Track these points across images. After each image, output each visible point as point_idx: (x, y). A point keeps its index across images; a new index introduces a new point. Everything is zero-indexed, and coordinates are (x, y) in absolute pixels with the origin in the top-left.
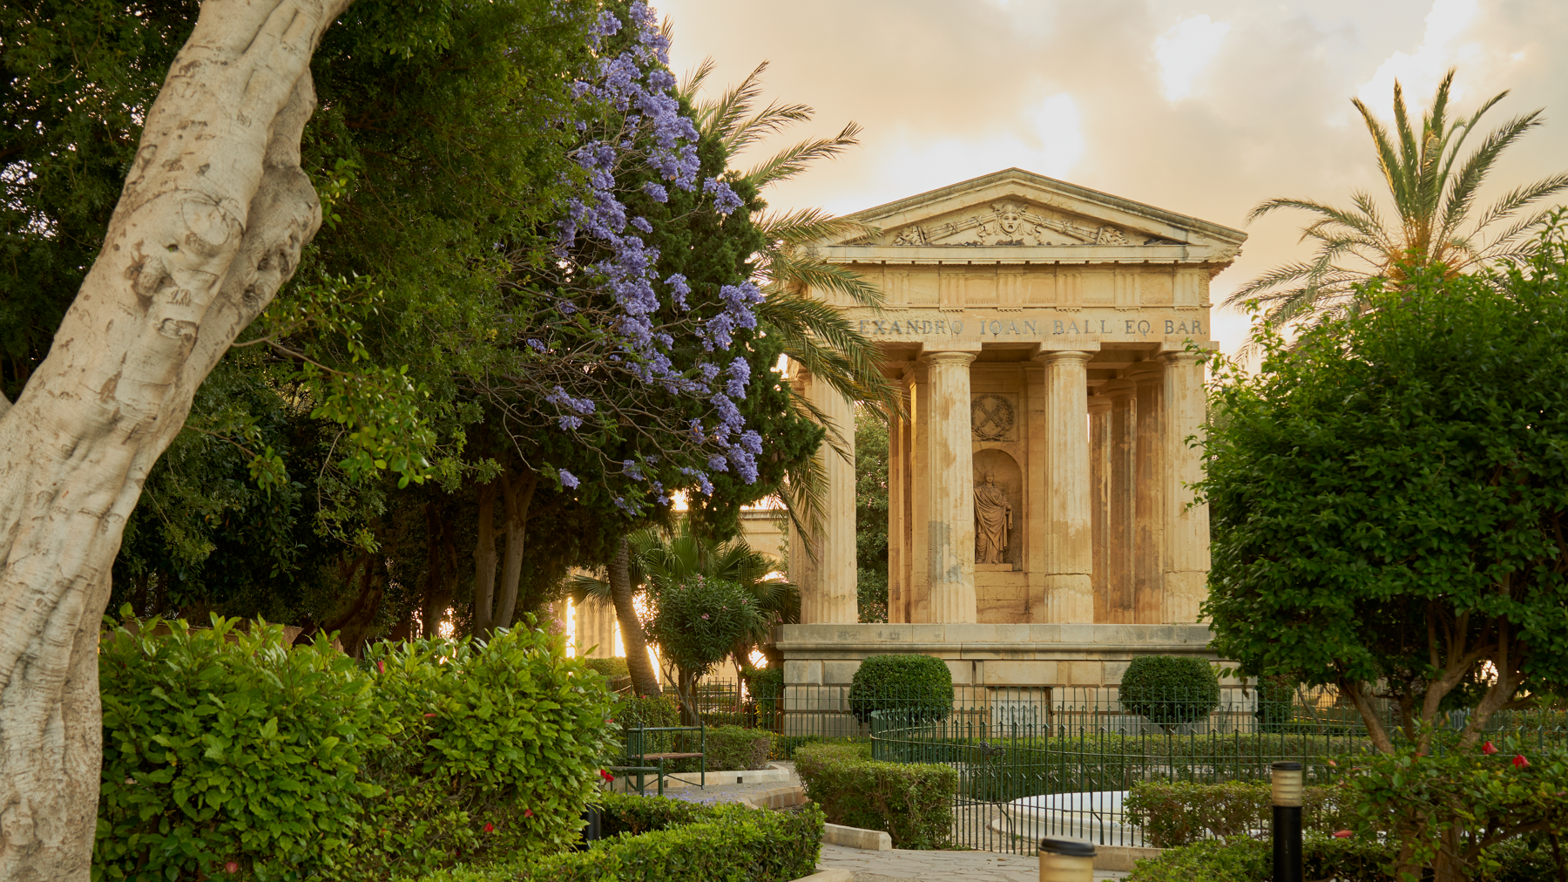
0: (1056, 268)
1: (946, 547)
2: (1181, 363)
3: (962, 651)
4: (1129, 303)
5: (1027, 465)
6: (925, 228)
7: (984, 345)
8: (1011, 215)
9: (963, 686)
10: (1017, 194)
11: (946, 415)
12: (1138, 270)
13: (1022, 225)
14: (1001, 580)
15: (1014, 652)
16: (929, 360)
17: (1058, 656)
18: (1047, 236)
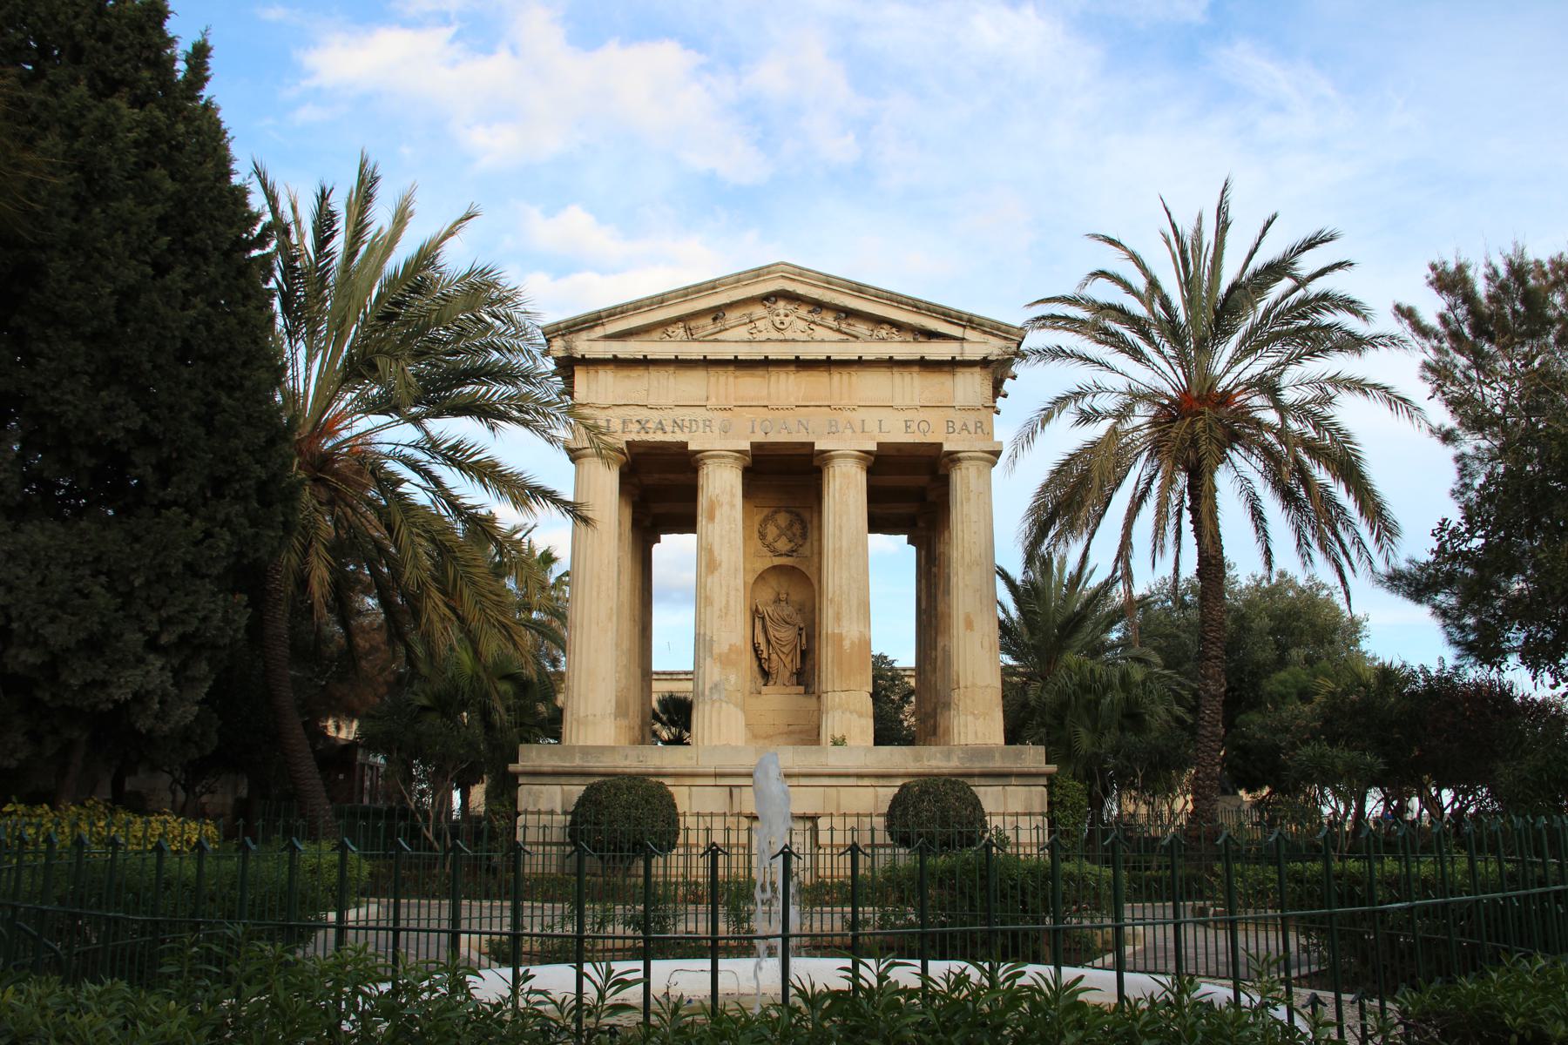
0: (828, 364)
2: (964, 464)
3: (716, 775)
4: (908, 402)
6: (693, 324)
7: (756, 446)
8: (782, 312)
9: (712, 814)
10: (786, 295)
11: (711, 518)
12: (916, 369)
13: (796, 321)
14: (778, 700)
16: (697, 461)
18: (820, 332)
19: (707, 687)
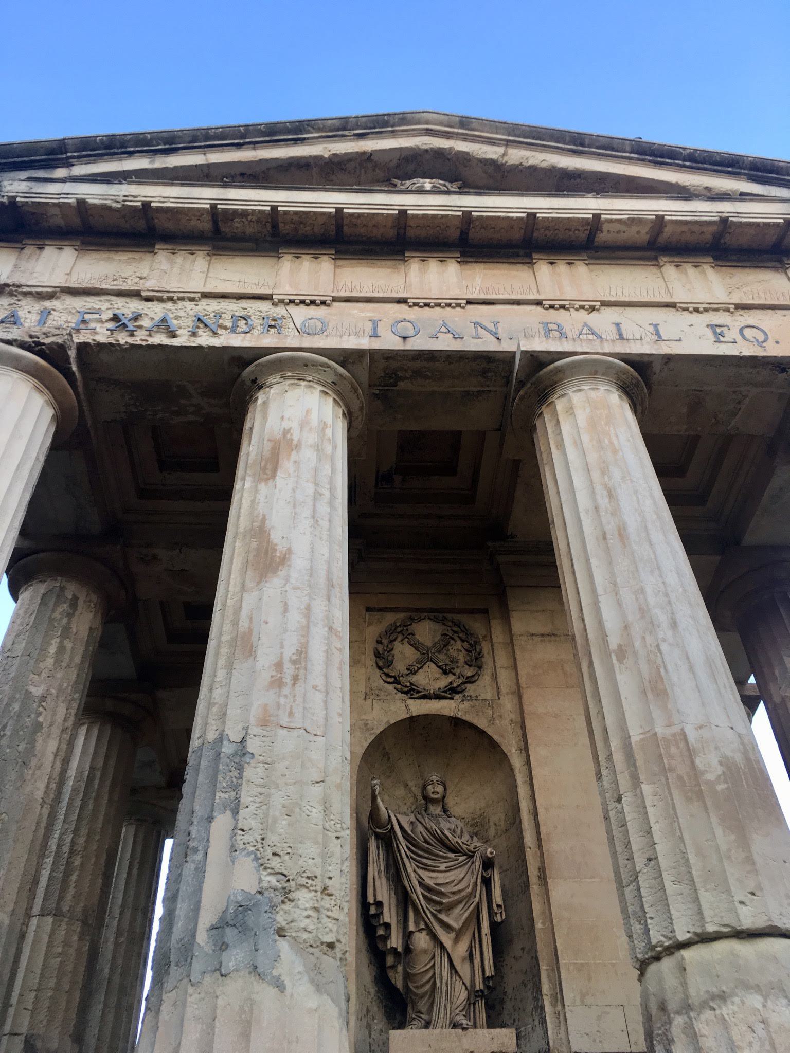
1: (222, 823)
5: (525, 749)
19: (207, 918)
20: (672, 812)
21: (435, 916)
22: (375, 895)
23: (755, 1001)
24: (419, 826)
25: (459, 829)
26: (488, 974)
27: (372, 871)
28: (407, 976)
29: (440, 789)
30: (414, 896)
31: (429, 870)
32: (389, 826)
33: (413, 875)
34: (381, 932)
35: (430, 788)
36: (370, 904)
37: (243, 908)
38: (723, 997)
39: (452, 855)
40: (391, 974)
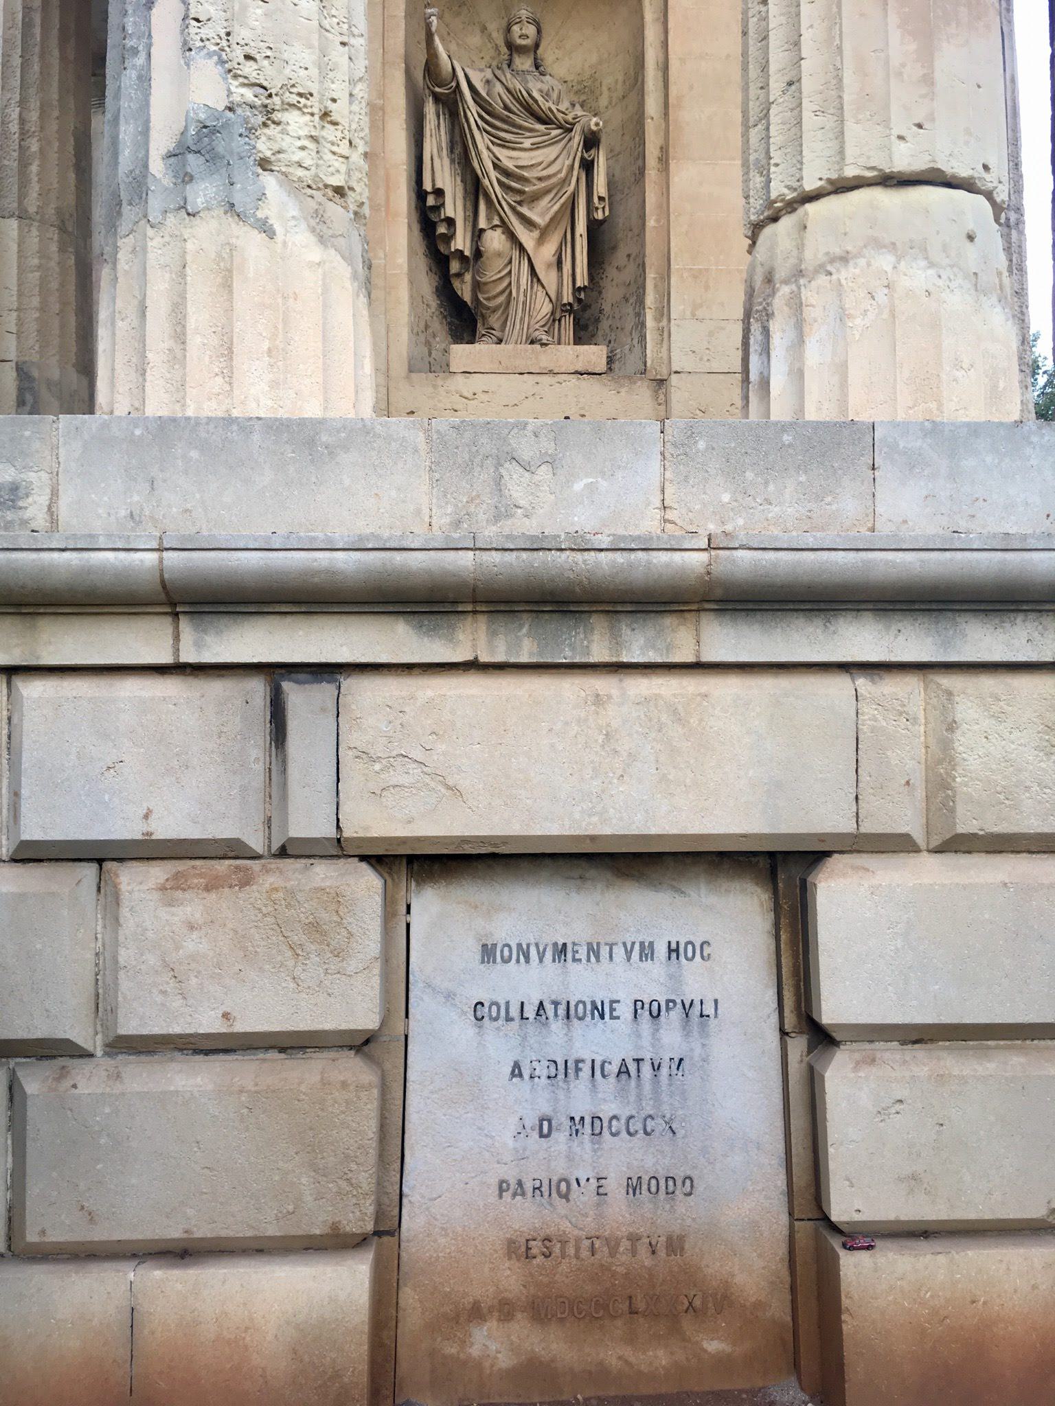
15: (554, 610)
17: (862, 639)
20: (835, 9)
21: (513, 209)
22: (433, 181)
23: (885, 262)
24: (498, 84)
25: (556, 92)
26: (579, 284)
27: (429, 147)
28: (477, 286)
29: (531, 30)
30: (486, 182)
31: (508, 148)
32: (454, 84)
33: (485, 154)
34: (442, 229)
35: (516, 28)
36: (427, 193)
37: (208, 130)
38: (844, 259)
39: (541, 127)
40: (456, 284)
